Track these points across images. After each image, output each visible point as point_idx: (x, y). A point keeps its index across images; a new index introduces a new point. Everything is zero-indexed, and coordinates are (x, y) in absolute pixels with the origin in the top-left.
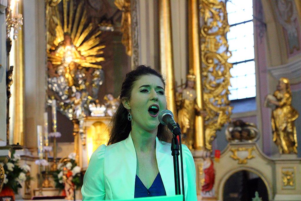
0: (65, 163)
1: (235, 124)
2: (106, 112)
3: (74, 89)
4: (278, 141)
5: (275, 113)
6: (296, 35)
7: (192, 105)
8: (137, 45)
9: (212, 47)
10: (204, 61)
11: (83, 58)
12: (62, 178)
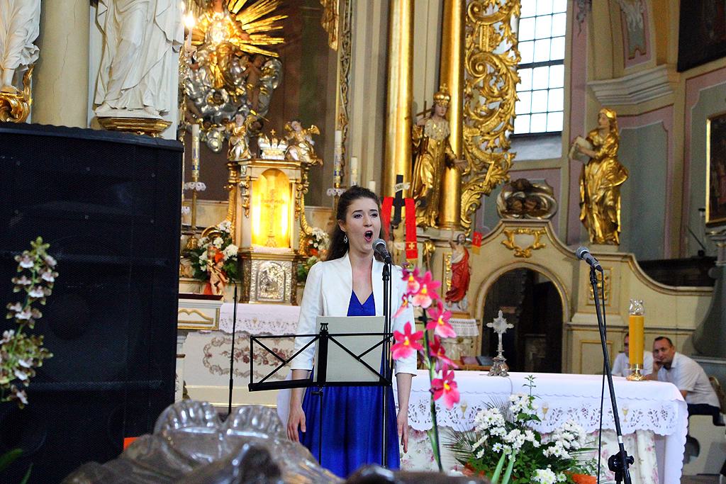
0: (212, 238)
1: (515, 187)
2: (286, 153)
3: (225, 95)
4: (589, 220)
5: (587, 169)
6: (641, 25)
7: (441, 148)
8: (348, 34)
9: (484, 43)
10: (468, 66)
11: (244, 36)
12: (205, 263)
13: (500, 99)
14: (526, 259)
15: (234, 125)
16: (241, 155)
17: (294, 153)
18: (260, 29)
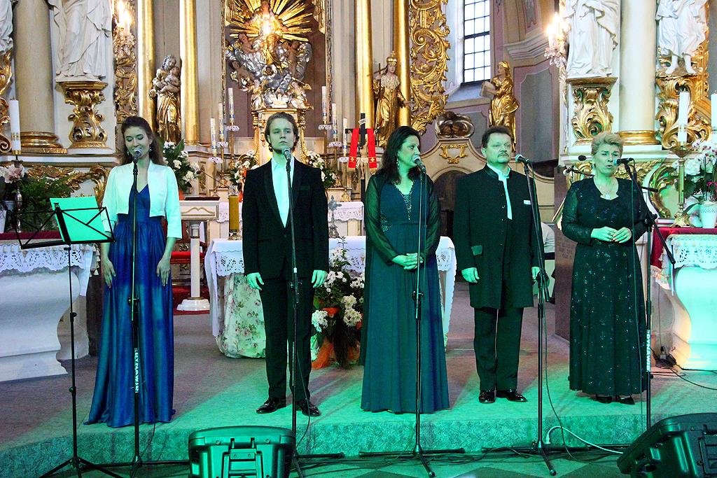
3: (274, 68)
6: (533, 4)
8: (329, 22)
11: (284, 28)
12: (238, 178)
13: (436, 59)
14: (456, 165)
15: (253, 86)
16: (259, 106)
17: (294, 103)
18: (296, 23)
